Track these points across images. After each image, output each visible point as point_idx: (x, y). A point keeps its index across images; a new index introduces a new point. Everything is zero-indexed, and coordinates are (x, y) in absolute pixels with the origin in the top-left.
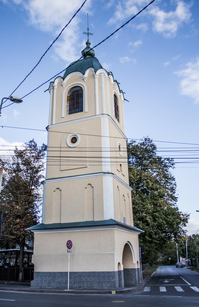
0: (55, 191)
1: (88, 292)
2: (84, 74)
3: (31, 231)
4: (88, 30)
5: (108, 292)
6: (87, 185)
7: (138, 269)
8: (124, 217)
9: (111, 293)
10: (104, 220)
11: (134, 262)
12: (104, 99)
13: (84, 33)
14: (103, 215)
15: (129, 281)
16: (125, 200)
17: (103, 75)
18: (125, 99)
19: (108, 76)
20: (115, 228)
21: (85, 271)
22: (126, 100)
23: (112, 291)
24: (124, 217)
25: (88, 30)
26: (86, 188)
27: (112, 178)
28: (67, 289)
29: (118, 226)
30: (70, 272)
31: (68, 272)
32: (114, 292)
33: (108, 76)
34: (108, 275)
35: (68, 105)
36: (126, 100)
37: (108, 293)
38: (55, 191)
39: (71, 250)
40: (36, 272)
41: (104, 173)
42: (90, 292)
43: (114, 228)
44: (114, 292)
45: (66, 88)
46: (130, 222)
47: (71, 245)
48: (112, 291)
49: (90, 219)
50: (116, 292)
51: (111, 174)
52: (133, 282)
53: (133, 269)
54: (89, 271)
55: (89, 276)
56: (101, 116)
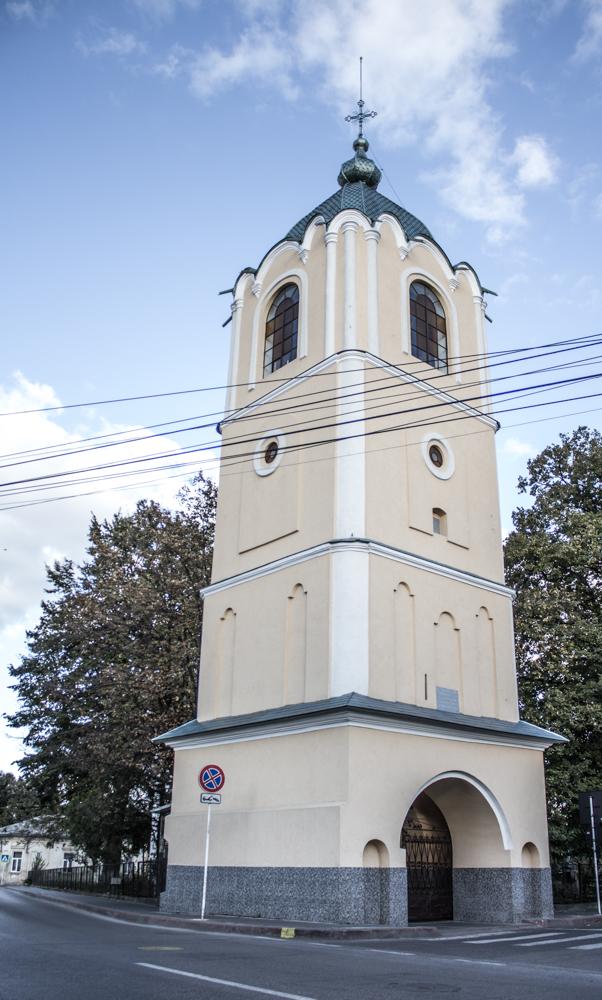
0: (223, 619)
1: (180, 922)
2: (301, 242)
3: (167, 744)
4: (361, 106)
5: (271, 930)
6: (291, 590)
7: (534, 873)
8: (439, 689)
9: (278, 932)
10: (329, 698)
11: (507, 846)
12: (351, 299)
13: (375, 114)
14: (327, 682)
15: (490, 910)
16: (457, 630)
17: (350, 228)
18: (483, 291)
19: (370, 228)
20: (350, 723)
21: (270, 865)
22: (488, 292)
23: (284, 929)
24: (439, 689)
25: (361, 106)
26: (291, 598)
27: (367, 556)
28: (200, 917)
29: (361, 716)
30: (208, 867)
31: (203, 868)
32: (288, 933)
33: (371, 229)
34: (326, 877)
35: (269, 345)
36: (488, 292)
37: (269, 934)
38: (223, 619)
39: (218, 797)
40: (175, 867)
41: (331, 543)
42: (227, 927)
43: (348, 721)
44: (288, 933)
45: (262, 298)
46: (508, 711)
47: (218, 780)
48: (284, 929)
49: (295, 700)
50: (296, 931)
51: (357, 544)
52: (503, 916)
53: (502, 870)
54: (281, 866)
55: (280, 882)
56: (337, 361)
